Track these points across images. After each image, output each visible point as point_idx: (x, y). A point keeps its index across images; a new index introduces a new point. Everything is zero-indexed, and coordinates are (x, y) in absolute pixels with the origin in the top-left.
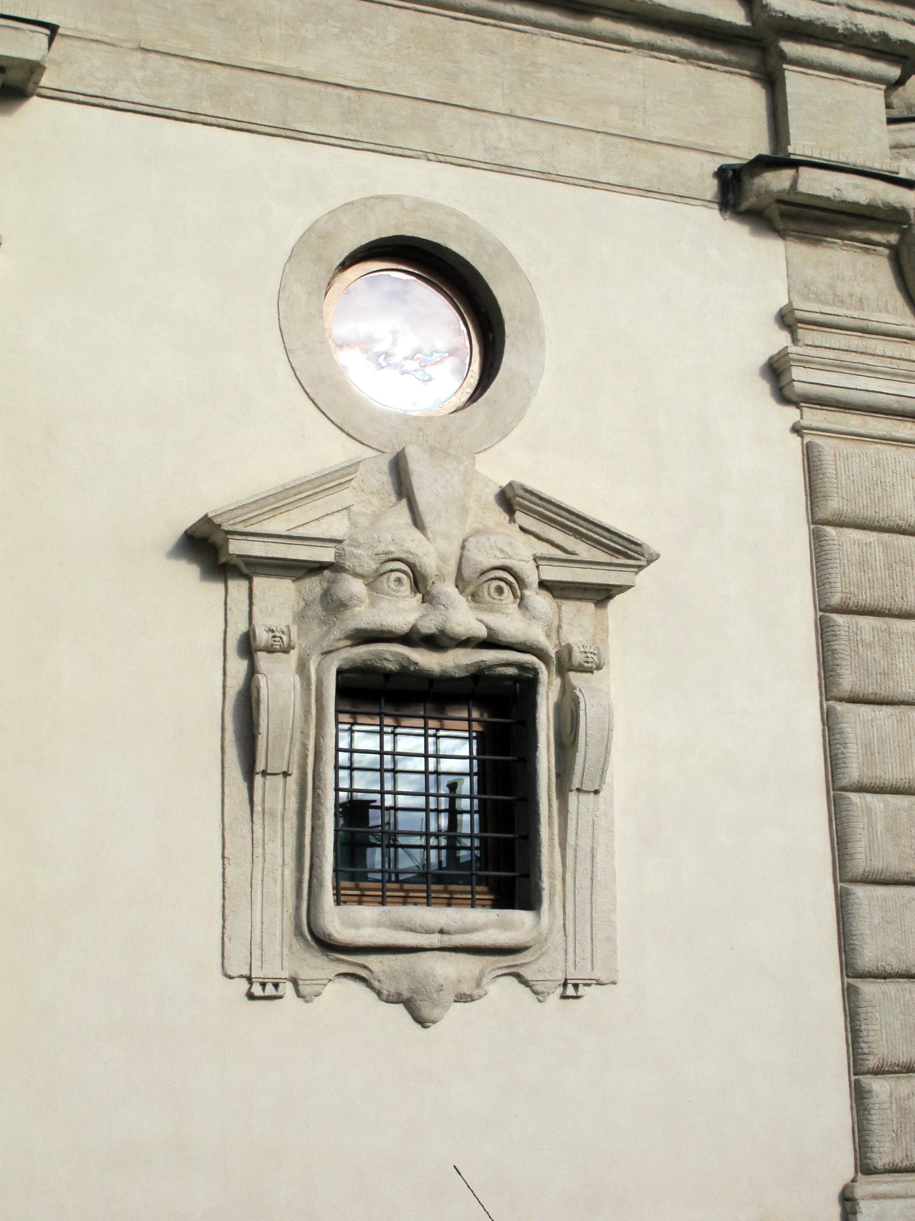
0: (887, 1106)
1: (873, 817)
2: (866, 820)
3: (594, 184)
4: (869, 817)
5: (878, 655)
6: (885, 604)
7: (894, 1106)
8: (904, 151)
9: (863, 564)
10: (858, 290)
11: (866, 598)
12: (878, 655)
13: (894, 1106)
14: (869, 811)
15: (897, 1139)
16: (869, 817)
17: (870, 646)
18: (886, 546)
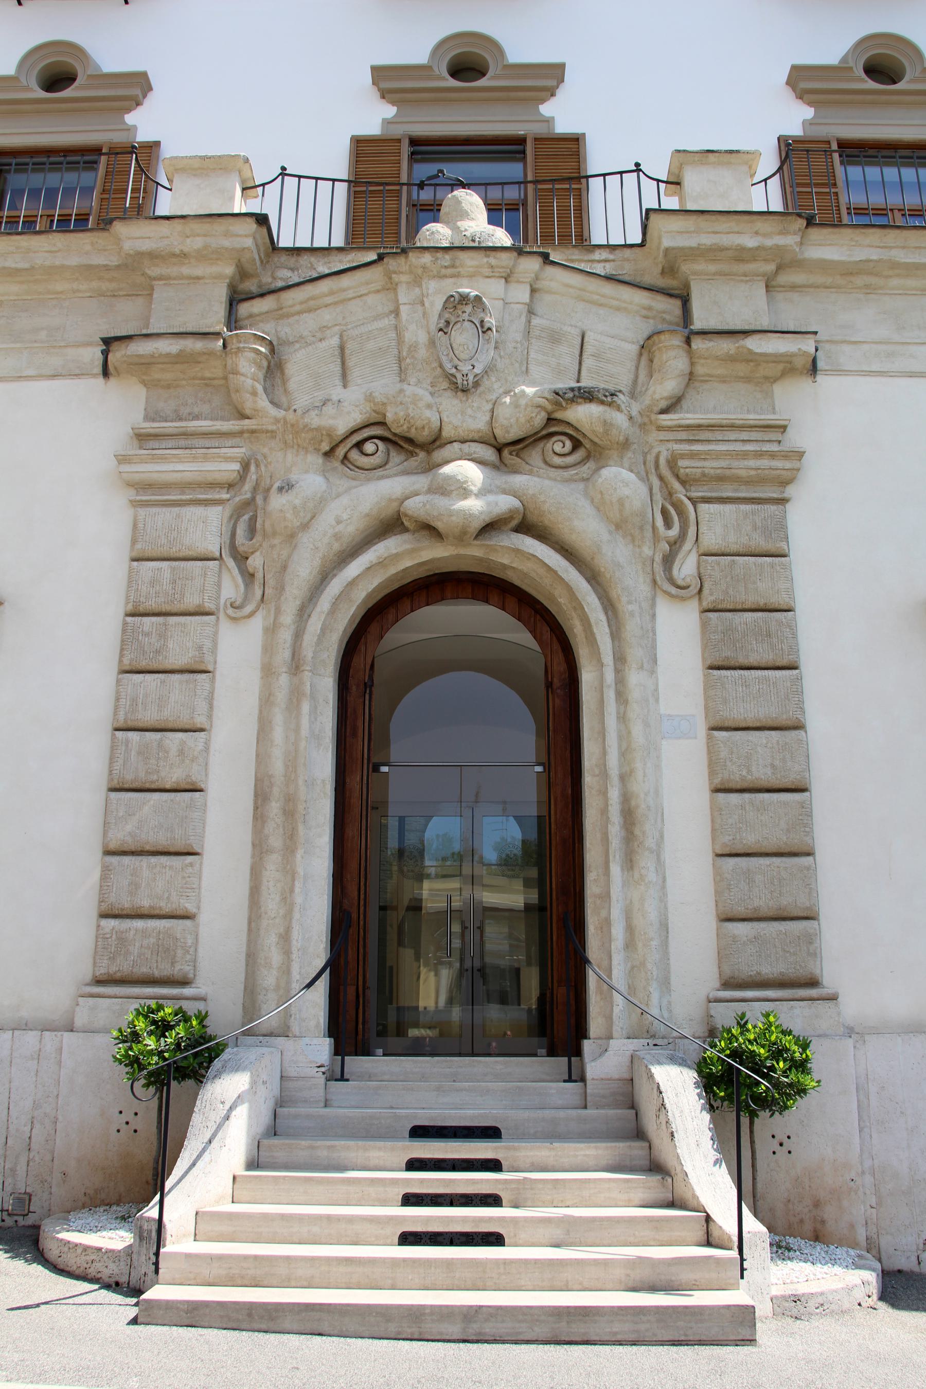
0: (108, 936)
1: (130, 745)
2: (124, 748)
3: (20, 378)
4: (127, 746)
5: (153, 640)
6: (166, 608)
7: (114, 936)
8: (258, 318)
9: (153, 583)
10: (196, 410)
11: (152, 604)
12: (154, 639)
13: (114, 936)
14: (127, 742)
15: (112, 959)
16: (127, 746)
17: (147, 634)
18: (173, 569)
